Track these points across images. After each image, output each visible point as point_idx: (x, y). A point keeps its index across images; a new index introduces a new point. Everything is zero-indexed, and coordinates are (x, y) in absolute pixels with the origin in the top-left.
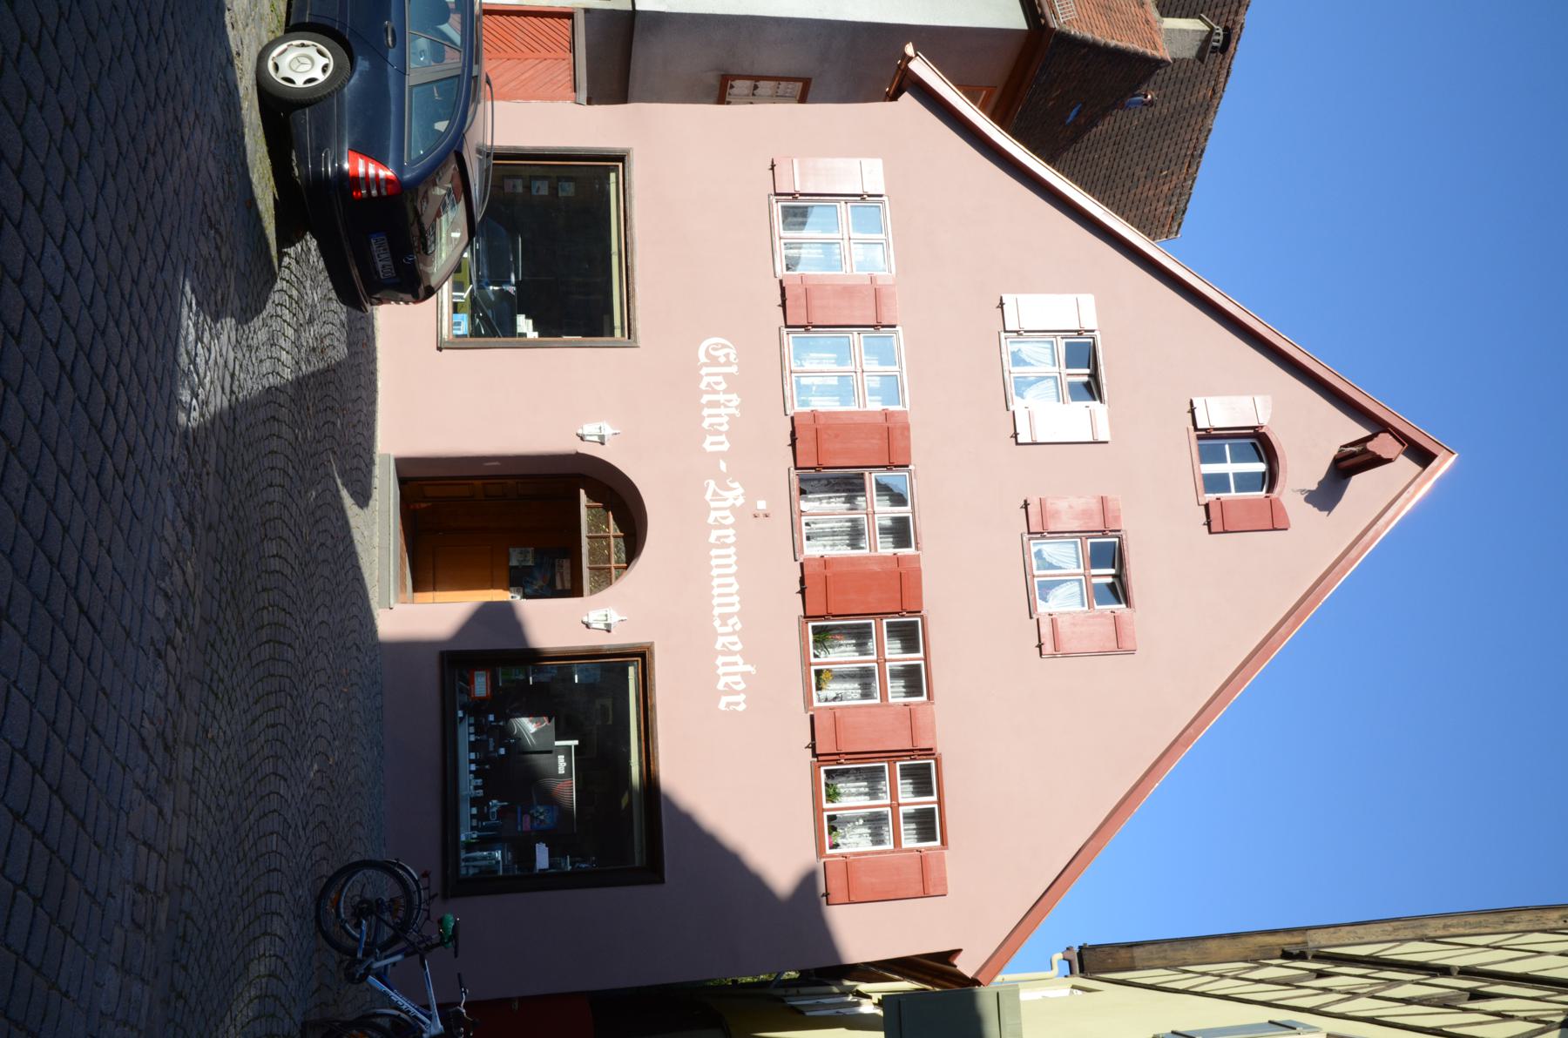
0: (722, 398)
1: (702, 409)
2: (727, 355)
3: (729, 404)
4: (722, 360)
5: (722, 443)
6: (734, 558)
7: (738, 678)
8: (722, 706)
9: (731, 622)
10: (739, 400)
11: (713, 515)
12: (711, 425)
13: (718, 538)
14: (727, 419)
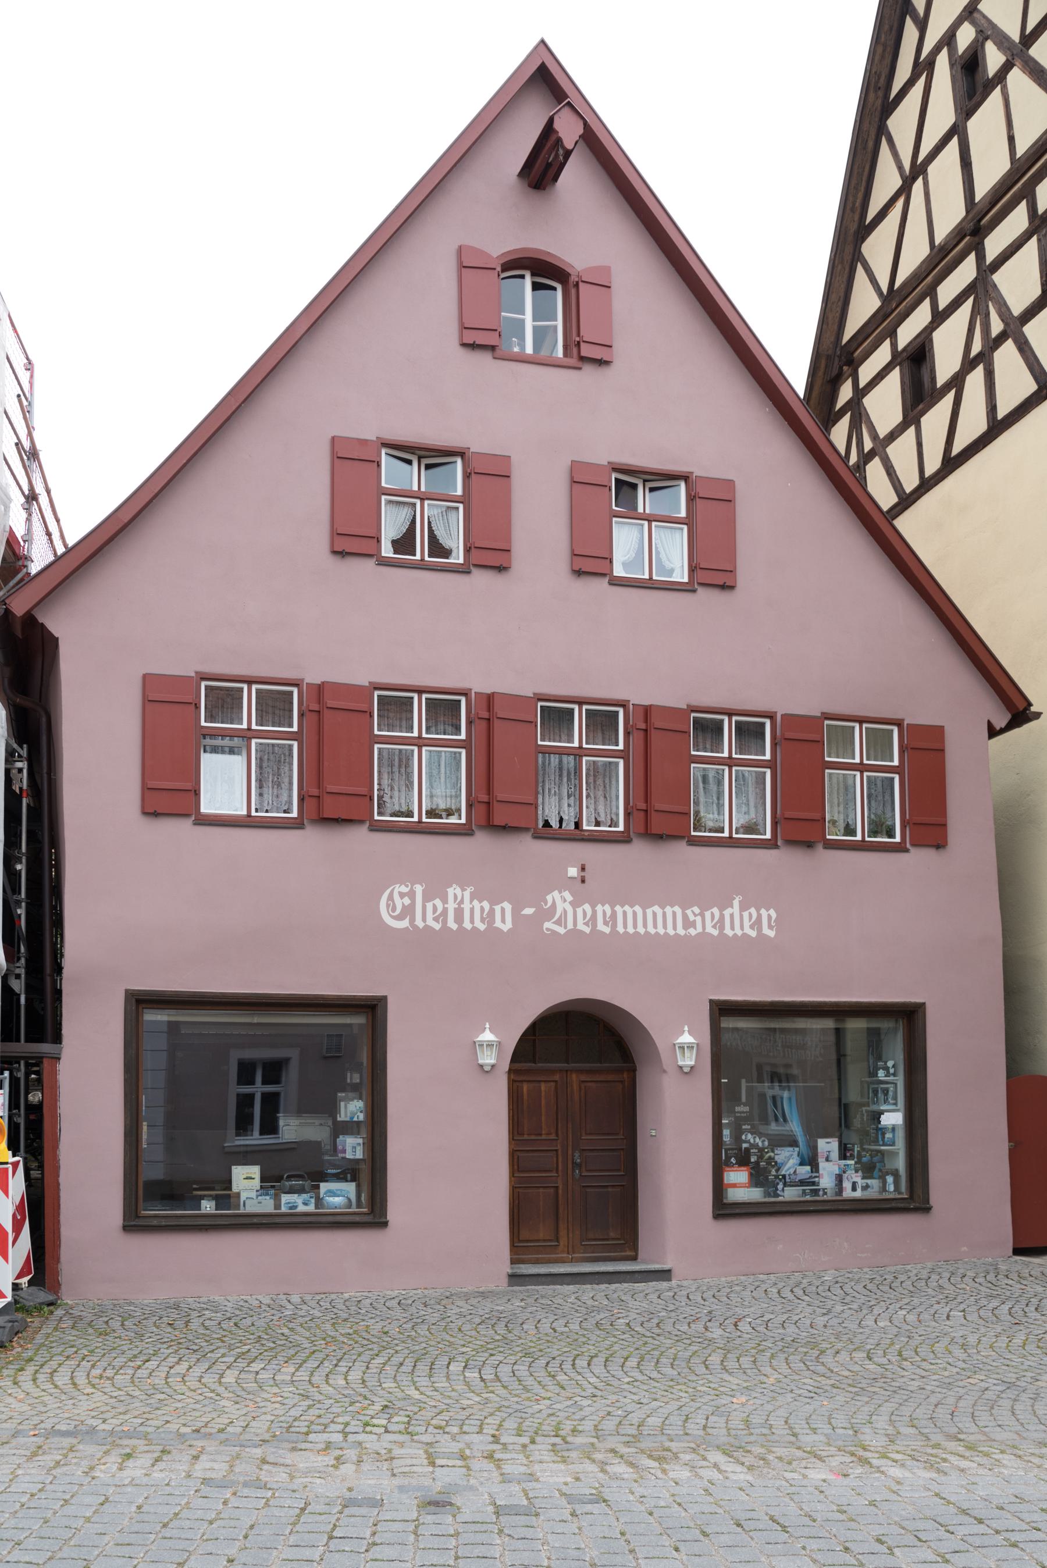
0: (451, 906)
1: (416, 927)
2: (402, 895)
3: (459, 898)
4: (407, 901)
5: (503, 910)
6: (627, 908)
7: (746, 914)
8: (771, 934)
9: (692, 918)
10: (454, 886)
11: (581, 926)
12: (482, 920)
13: (606, 923)
14: (476, 902)
